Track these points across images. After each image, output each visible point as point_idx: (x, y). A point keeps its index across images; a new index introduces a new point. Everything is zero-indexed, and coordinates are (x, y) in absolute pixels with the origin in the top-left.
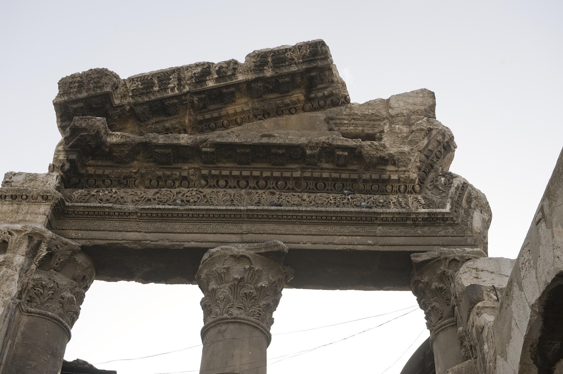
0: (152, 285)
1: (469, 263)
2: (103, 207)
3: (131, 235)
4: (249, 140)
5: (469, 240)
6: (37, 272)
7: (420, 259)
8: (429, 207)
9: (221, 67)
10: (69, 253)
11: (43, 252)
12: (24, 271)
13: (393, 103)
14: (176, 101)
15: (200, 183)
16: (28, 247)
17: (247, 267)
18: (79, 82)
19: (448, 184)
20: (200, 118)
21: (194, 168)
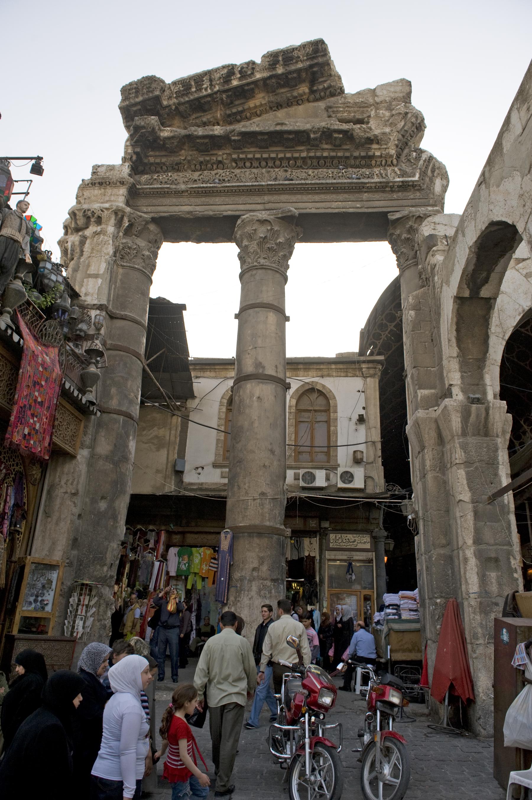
0: (203, 244)
1: (429, 219)
2: (163, 188)
3: (185, 208)
4: (267, 128)
5: (431, 201)
6: (124, 238)
7: (394, 217)
8: (403, 177)
9: (242, 68)
10: (144, 223)
11: (126, 224)
12: (115, 237)
13: (378, 92)
14: (209, 99)
15: (232, 165)
16: (115, 220)
17: (269, 228)
18: (135, 88)
19: (418, 158)
20: (228, 112)
21: (226, 154)
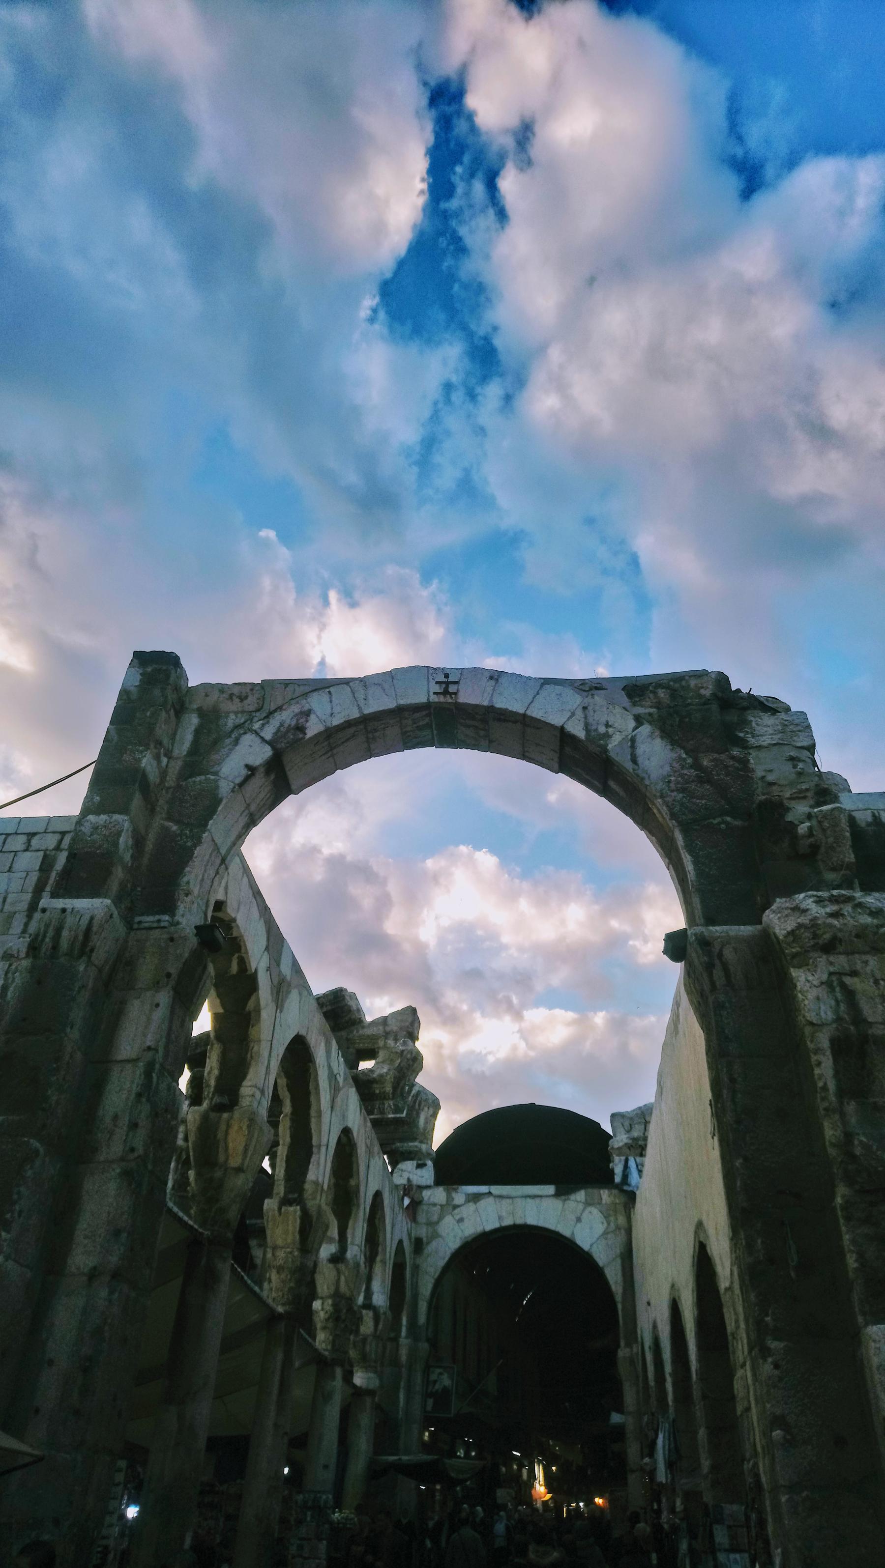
13: (389, 1022)
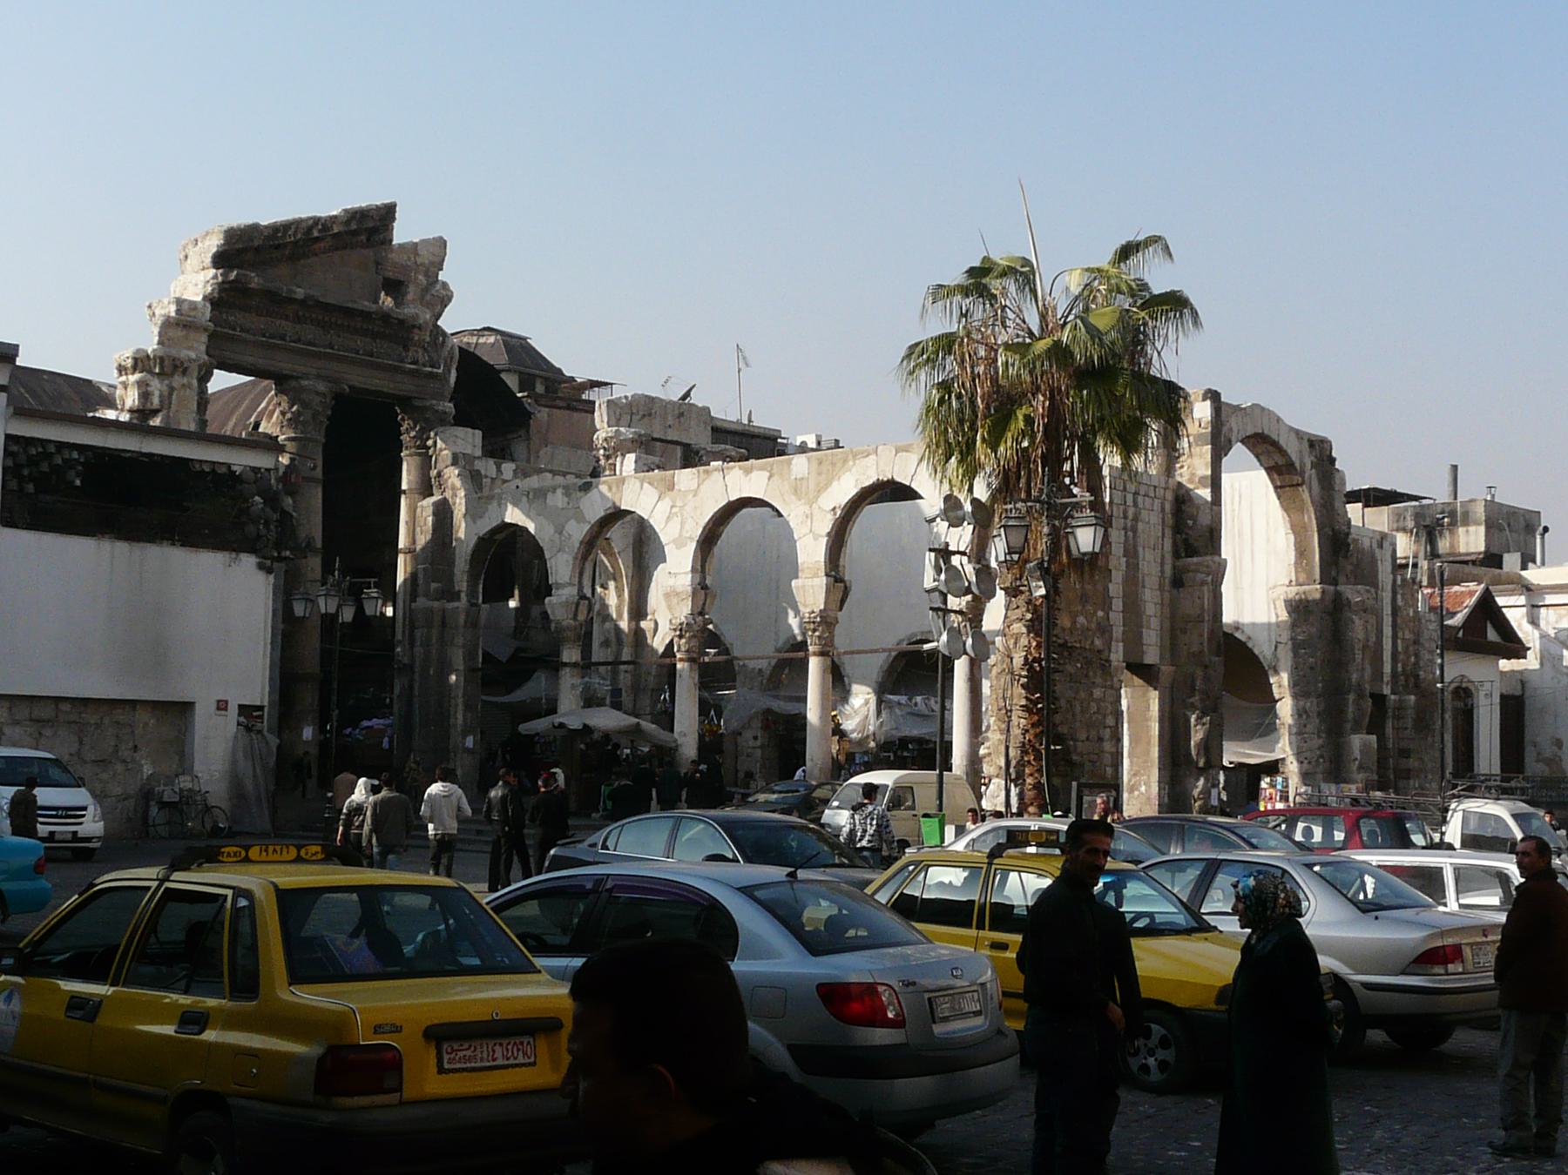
13: (422, 251)
